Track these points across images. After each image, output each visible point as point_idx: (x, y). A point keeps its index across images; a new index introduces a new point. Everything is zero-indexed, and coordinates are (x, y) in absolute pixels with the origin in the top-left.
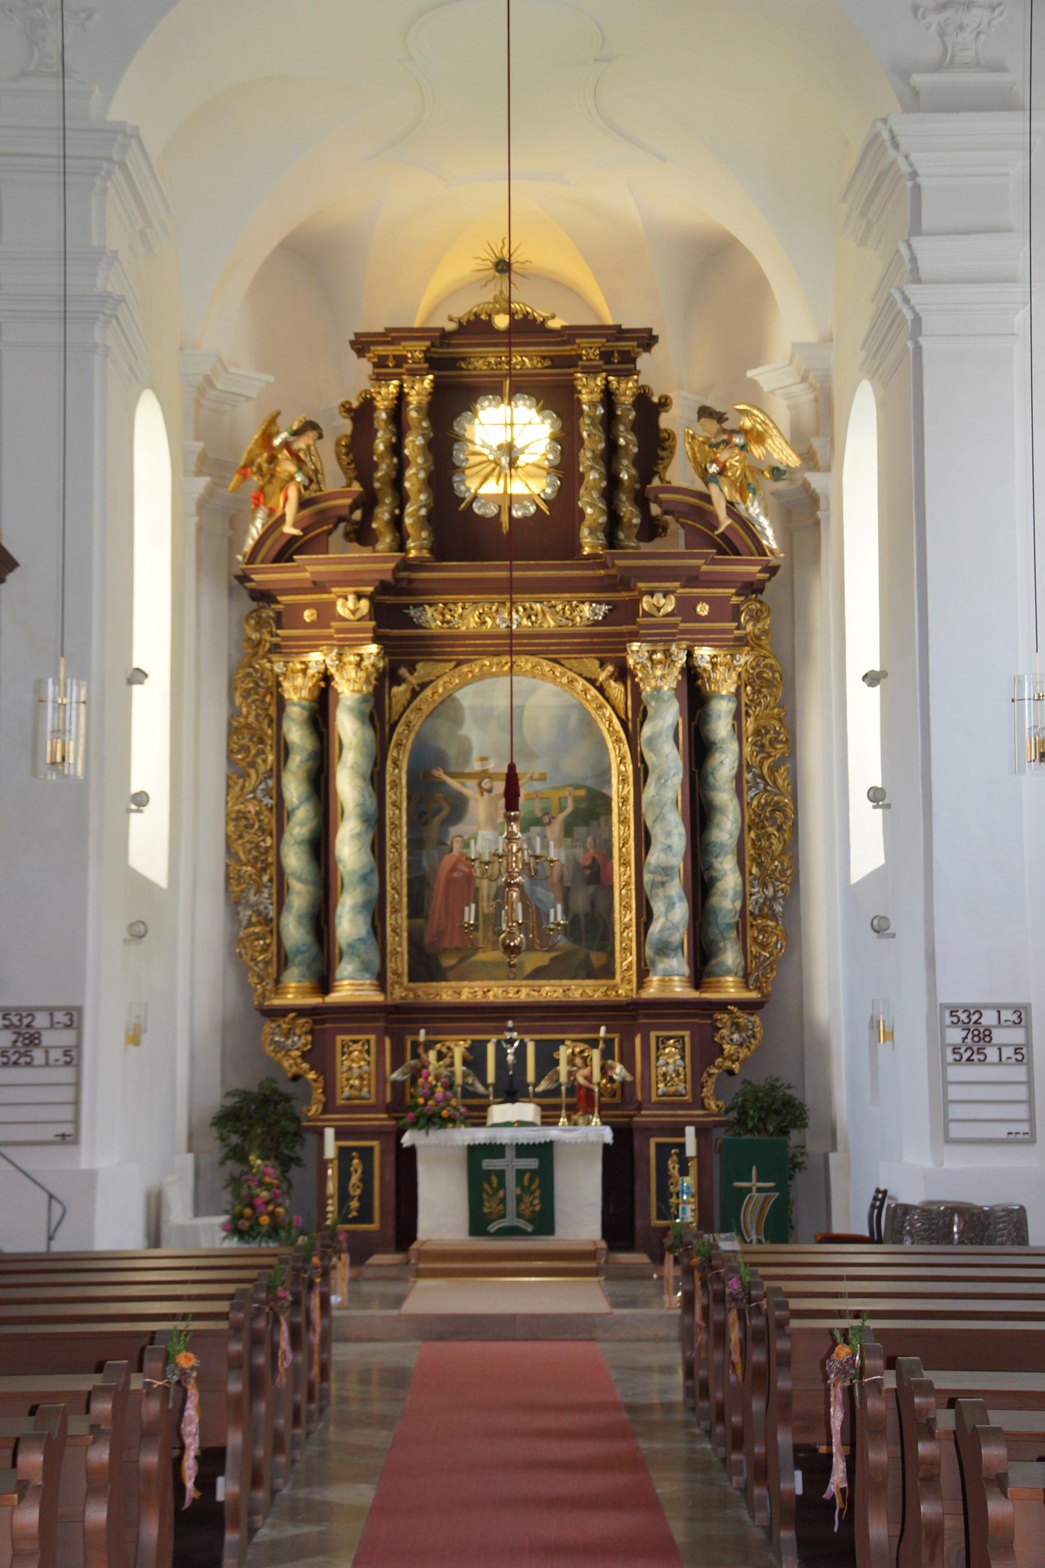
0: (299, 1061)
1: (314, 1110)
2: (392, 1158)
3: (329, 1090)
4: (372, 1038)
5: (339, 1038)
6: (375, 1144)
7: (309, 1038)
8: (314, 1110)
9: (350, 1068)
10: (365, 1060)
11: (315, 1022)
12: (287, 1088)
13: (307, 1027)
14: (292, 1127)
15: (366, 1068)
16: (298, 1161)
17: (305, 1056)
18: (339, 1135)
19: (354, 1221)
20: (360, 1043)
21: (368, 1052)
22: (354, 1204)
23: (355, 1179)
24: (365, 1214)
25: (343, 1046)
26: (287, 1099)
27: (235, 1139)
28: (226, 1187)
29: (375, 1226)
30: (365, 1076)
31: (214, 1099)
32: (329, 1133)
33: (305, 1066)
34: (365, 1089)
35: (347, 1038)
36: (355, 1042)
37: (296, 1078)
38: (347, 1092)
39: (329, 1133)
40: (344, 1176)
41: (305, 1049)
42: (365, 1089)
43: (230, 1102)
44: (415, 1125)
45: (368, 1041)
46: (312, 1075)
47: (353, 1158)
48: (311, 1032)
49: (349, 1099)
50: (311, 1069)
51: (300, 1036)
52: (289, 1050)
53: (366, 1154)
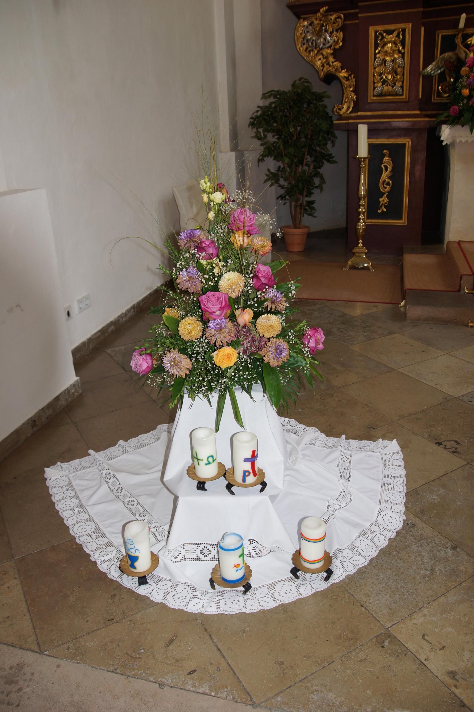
0: (331, 59)
1: (345, 109)
2: (422, 156)
3: (360, 89)
4: (408, 27)
5: (372, 30)
6: (407, 141)
7: (341, 35)
8: (345, 109)
9: (384, 62)
10: (399, 52)
11: (347, 17)
12: (318, 87)
13: (340, 22)
14: (324, 126)
15: (399, 61)
16: (329, 158)
17: (336, 54)
18: (371, 133)
19: (383, 216)
20: (395, 34)
21: (403, 43)
22: (384, 200)
23: (385, 176)
24: (394, 210)
25: (376, 38)
26: (320, 97)
27: (271, 138)
28: (266, 181)
29: (403, 222)
30: (399, 70)
31: (252, 102)
32: (363, 130)
33: (337, 64)
34: (398, 84)
35: (381, 28)
36: (390, 32)
37: (330, 78)
38: (379, 88)
39: (363, 130)
40: (375, 174)
41: (337, 47)
42: (398, 84)
43: (267, 102)
44: (454, 121)
45: (404, 31)
46: (343, 74)
47: (384, 156)
48: (343, 29)
49: (381, 95)
50: (342, 68)
51: (332, 33)
52: (322, 49)
53: (397, 152)
